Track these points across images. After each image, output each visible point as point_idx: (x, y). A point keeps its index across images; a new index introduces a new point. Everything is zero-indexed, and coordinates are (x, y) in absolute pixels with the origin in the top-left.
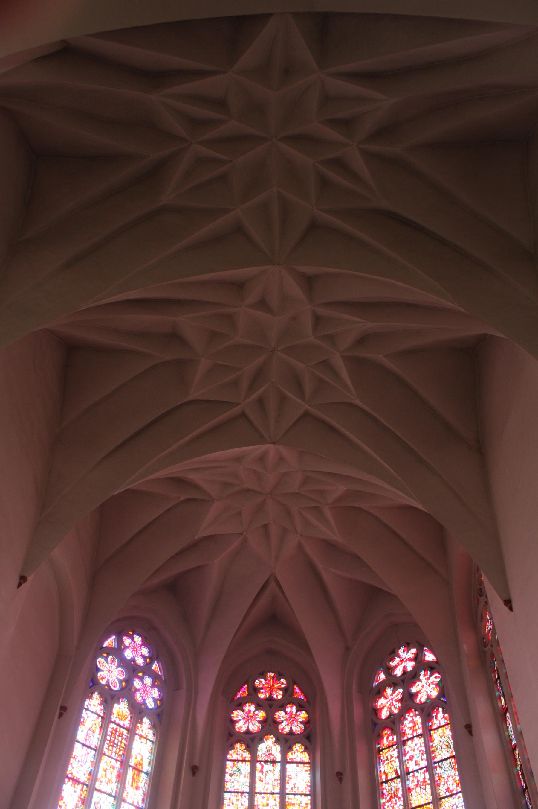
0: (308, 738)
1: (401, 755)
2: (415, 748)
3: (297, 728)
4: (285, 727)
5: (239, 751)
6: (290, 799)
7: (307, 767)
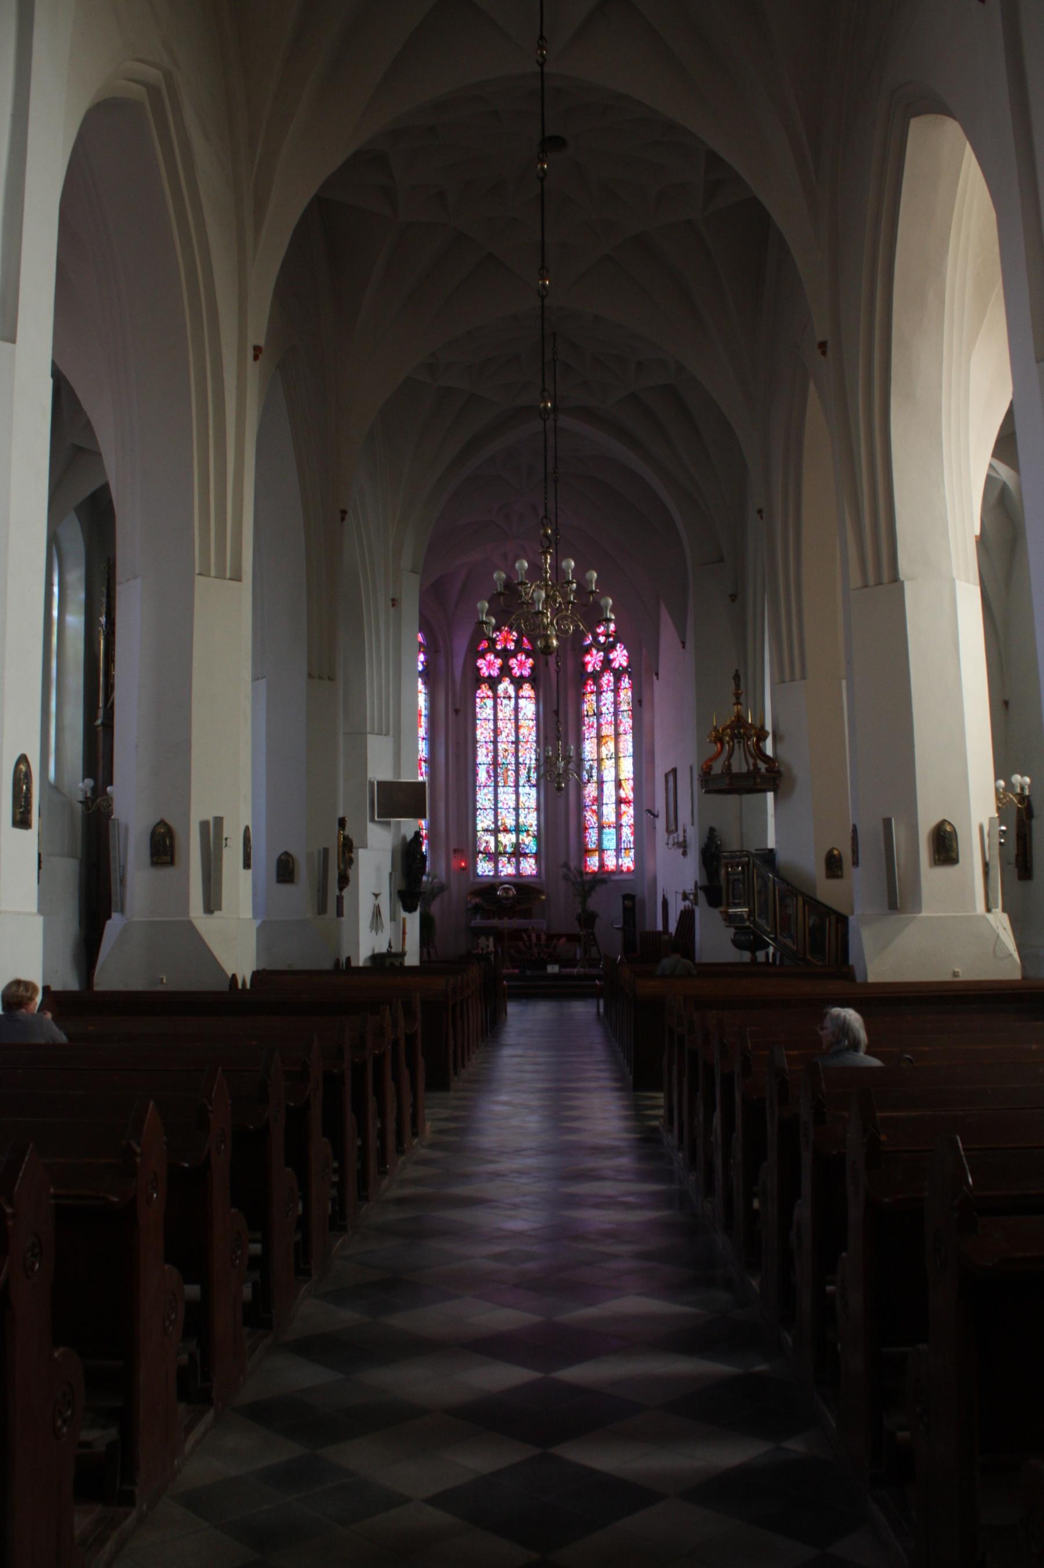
0: (534, 680)
1: (598, 701)
2: (608, 697)
3: (526, 673)
4: (517, 672)
5: (484, 691)
6: (521, 723)
7: (533, 701)
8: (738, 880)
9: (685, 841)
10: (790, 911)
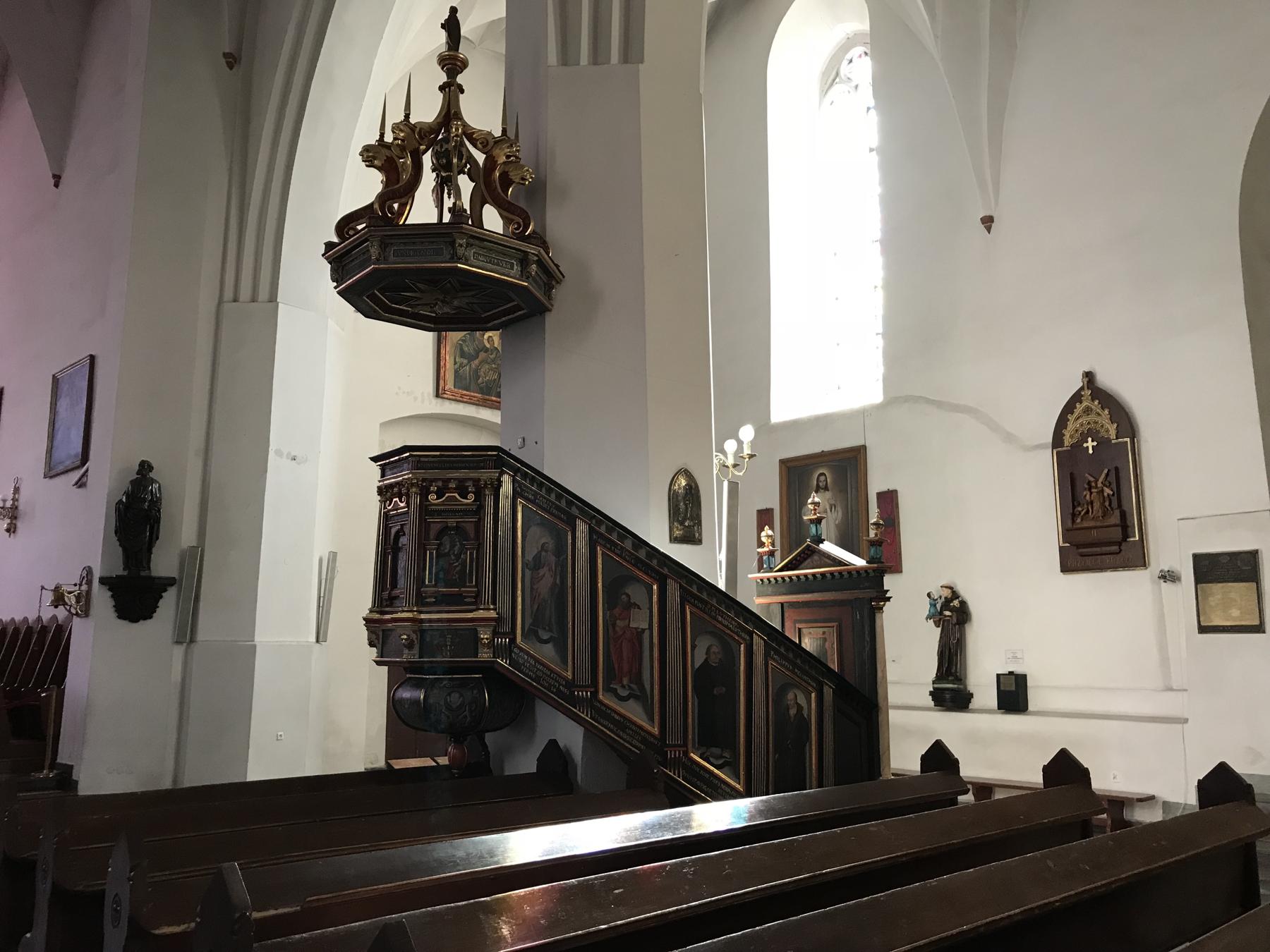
8: (458, 528)
9: (15, 508)
10: (639, 621)
